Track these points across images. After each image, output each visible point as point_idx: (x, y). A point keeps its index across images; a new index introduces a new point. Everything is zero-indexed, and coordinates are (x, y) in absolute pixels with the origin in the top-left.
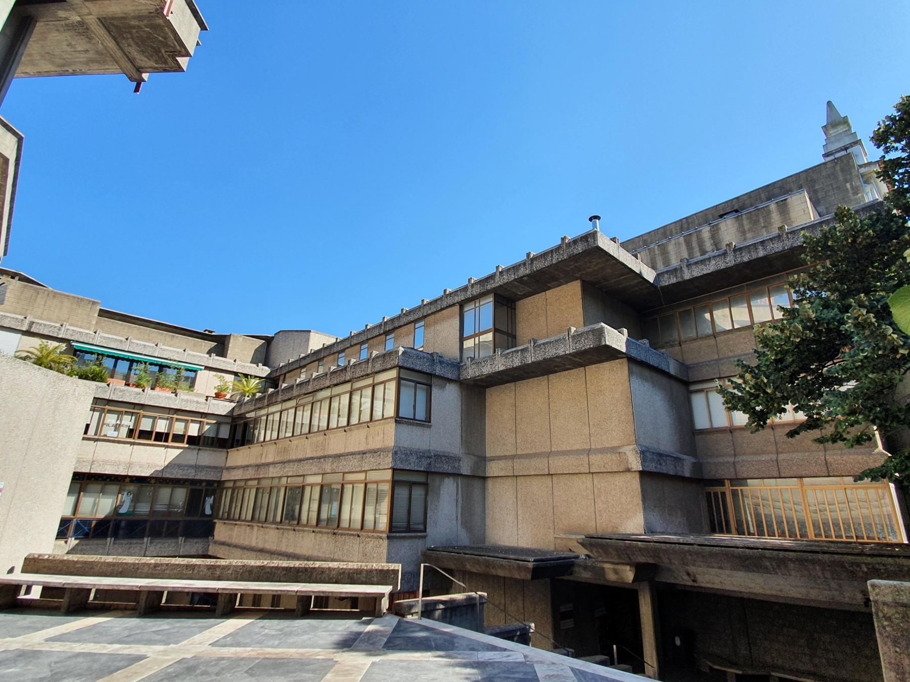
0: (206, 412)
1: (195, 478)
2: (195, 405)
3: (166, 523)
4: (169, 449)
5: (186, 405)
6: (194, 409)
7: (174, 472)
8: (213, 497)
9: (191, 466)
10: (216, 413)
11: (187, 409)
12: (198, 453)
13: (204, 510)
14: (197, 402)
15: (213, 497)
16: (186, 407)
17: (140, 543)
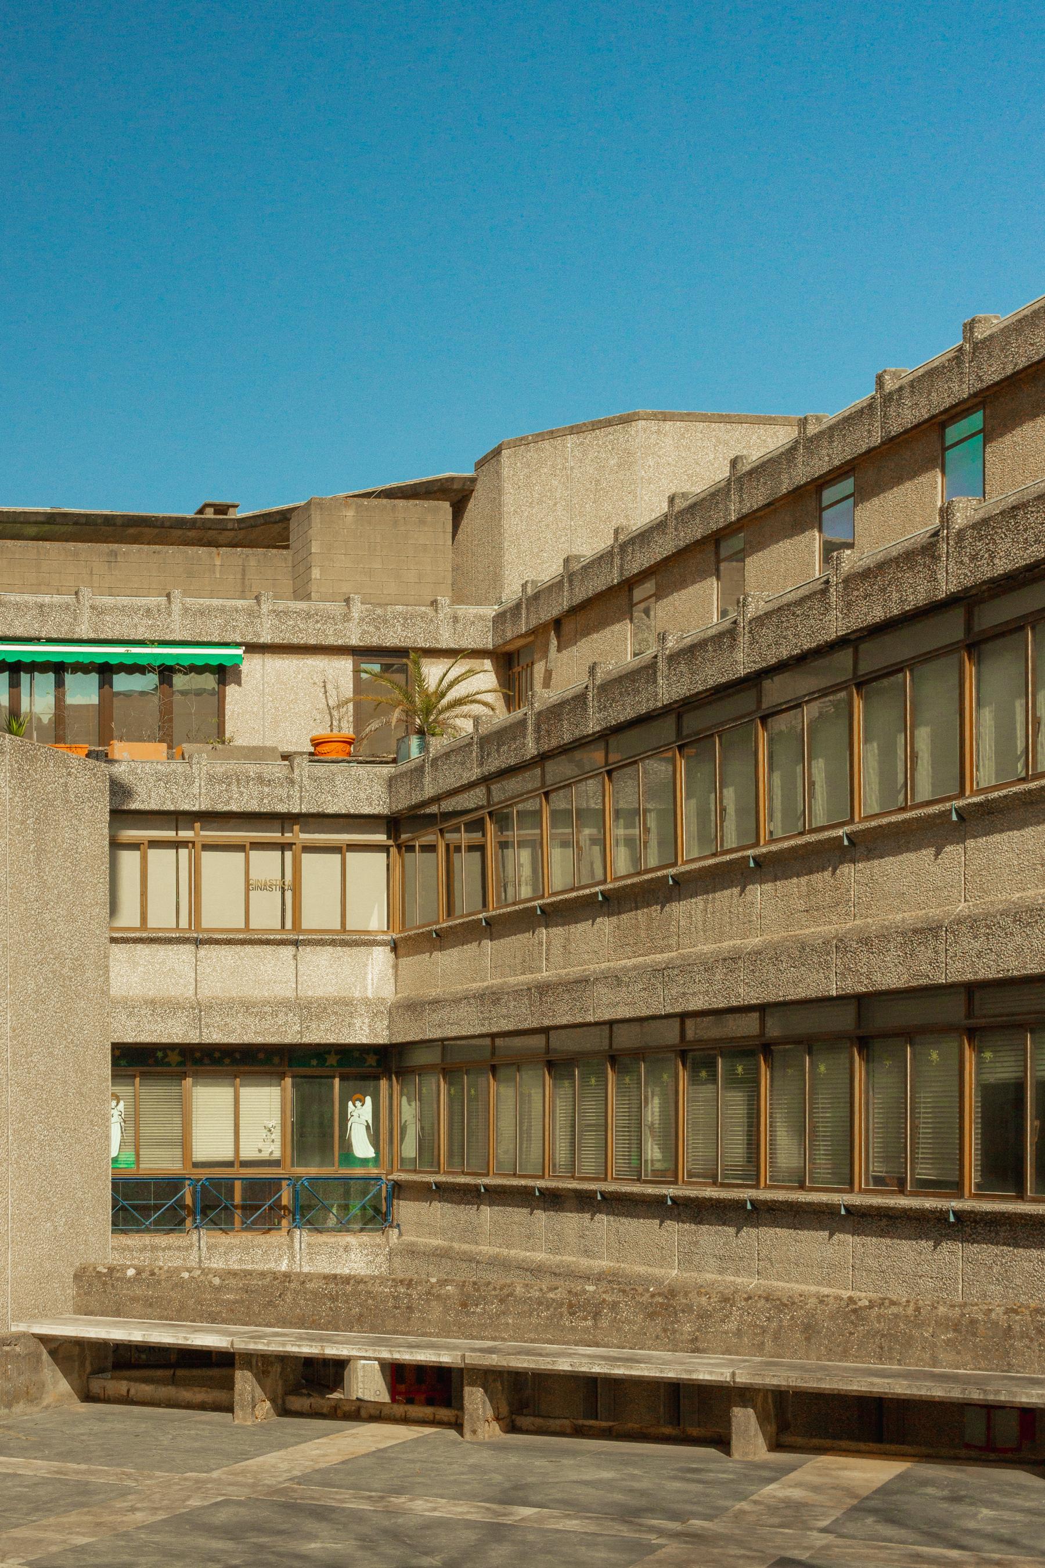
0: (296, 811)
1: (306, 1040)
2: (255, 789)
3: (238, 1184)
4: (204, 951)
5: (226, 795)
6: (253, 806)
7: (234, 1023)
8: (368, 1100)
9: (286, 1005)
10: (331, 810)
11: (234, 807)
12: (295, 957)
13: (346, 1145)
14: (260, 779)
15: (368, 1100)
16: (228, 803)
17: (179, 1248)
